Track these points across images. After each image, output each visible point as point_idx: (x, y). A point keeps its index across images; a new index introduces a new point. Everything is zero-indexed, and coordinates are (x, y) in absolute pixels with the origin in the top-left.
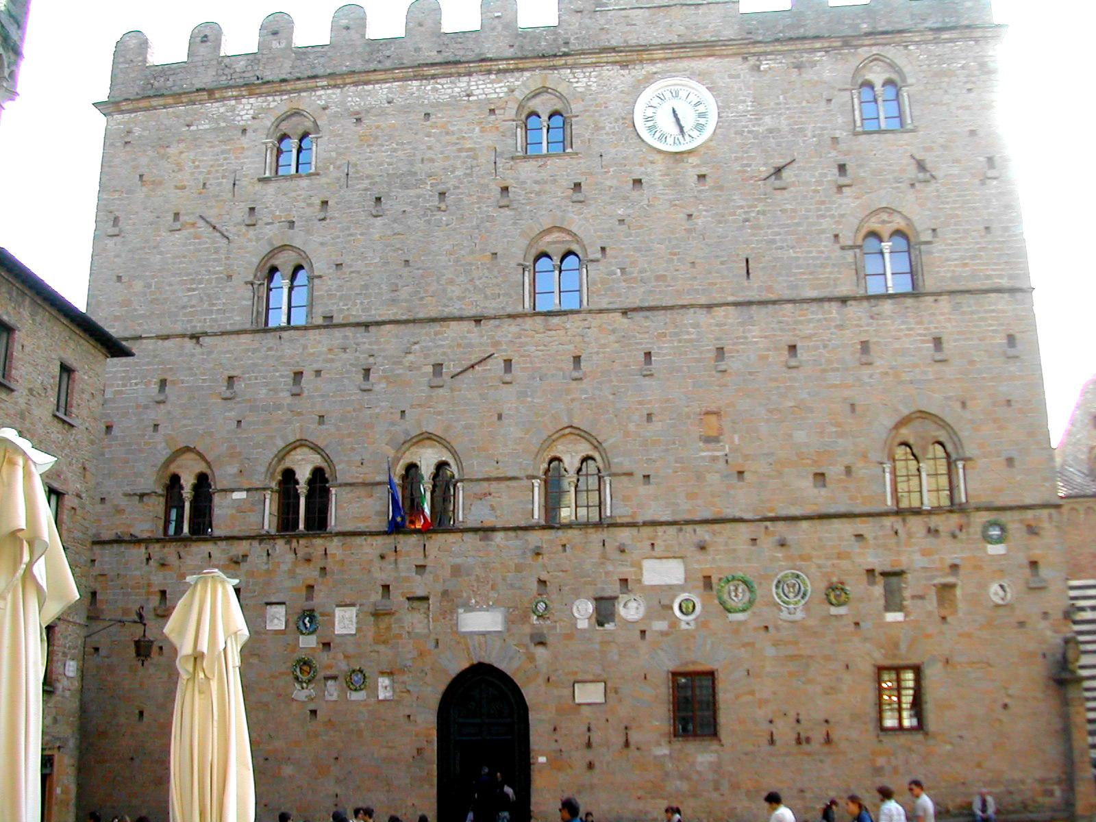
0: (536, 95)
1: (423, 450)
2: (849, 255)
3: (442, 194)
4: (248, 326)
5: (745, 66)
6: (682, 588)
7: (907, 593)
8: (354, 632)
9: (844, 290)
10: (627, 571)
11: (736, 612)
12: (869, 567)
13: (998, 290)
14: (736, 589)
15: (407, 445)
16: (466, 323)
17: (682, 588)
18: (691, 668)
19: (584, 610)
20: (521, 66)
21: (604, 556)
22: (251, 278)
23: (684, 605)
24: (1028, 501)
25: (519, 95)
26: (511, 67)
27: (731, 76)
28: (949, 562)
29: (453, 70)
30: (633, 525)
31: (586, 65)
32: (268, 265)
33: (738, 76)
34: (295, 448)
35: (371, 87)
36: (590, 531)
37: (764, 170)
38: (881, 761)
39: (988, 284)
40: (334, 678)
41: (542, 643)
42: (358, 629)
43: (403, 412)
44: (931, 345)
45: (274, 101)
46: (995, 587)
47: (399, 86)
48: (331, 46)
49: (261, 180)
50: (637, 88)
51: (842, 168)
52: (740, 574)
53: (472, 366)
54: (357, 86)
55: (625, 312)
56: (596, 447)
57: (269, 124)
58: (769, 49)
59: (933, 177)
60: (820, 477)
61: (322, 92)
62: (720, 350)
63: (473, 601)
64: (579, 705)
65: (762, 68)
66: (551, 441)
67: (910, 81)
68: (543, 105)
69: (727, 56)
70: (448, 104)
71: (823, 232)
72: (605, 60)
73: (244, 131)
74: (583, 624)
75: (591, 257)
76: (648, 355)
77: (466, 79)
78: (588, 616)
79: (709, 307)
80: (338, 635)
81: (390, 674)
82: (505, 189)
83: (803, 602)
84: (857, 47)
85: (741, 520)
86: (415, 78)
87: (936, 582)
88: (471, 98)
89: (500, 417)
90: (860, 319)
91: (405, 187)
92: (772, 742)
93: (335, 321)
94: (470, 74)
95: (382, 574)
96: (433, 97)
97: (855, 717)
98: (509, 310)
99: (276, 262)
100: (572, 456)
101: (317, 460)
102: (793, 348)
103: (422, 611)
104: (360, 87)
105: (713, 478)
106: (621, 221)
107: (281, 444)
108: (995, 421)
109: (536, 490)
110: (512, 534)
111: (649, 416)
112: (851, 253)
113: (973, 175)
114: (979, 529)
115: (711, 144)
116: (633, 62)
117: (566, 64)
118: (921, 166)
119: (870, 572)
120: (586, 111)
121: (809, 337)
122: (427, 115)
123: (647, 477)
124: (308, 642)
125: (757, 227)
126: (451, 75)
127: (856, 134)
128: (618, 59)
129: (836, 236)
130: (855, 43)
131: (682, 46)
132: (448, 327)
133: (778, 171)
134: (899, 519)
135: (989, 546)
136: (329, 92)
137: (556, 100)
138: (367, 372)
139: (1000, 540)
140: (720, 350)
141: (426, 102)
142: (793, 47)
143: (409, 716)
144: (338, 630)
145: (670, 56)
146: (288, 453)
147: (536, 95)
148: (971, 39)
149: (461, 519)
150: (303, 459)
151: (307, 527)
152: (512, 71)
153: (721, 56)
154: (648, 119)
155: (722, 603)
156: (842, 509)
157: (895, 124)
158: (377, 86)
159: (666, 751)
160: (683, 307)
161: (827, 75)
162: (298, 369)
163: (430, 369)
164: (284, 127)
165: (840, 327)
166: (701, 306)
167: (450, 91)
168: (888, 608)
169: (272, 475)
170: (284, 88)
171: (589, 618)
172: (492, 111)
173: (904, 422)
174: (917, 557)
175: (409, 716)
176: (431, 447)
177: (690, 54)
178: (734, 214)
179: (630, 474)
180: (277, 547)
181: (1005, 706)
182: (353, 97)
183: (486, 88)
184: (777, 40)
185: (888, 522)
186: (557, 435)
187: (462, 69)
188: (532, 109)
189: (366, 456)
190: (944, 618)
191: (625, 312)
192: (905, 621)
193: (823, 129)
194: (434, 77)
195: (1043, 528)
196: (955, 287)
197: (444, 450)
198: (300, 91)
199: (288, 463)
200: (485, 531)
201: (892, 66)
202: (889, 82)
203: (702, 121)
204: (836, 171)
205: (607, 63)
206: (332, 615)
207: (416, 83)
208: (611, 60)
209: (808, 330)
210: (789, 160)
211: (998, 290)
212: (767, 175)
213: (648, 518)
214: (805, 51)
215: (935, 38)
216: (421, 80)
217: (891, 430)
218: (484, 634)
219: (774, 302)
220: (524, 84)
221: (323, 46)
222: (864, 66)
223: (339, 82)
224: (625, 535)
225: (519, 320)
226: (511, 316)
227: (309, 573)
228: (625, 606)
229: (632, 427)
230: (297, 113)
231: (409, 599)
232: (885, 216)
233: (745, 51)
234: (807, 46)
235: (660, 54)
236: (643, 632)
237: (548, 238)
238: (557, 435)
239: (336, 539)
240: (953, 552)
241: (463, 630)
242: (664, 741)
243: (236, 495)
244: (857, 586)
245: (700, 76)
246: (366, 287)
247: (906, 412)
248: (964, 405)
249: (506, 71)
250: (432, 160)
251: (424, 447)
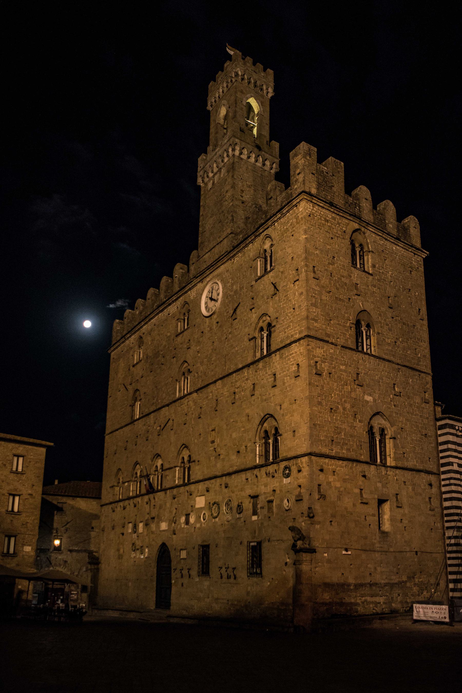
2: (252, 342)
7: (259, 506)
13: (295, 342)
19: (183, 519)
21: (188, 498)
24: (299, 453)
28: (272, 489)
37: (232, 312)
38: (249, 588)
39: (292, 339)
40: (138, 549)
46: (286, 501)
53: (166, 425)
55: (196, 391)
58: (235, 252)
72: (196, 282)
74: (183, 526)
79: (215, 382)
87: (268, 499)
92: (222, 577)
105: (212, 458)
109: (177, 472)
112: (252, 341)
114: (282, 471)
123: (198, 461)
124: (135, 536)
127: (256, 281)
133: (235, 310)
134: (258, 469)
135: (284, 479)
139: (288, 476)
156: (243, 467)
165: (247, 379)
174: (263, 487)
177: (215, 268)
179: (194, 461)
185: (256, 471)
190: (270, 517)
191: (196, 391)
192: (258, 520)
195: (303, 467)
196: (281, 345)
200: (165, 490)
206: (138, 526)
208: (197, 281)
211: (295, 342)
213: (197, 479)
217: (259, 425)
218: (164, 531)
224: (193, 487)
226: (175, 401)
232: (264, 318)
233: (229, 257)
235: (208, 272)
240: (274, 484)
243: (126, 484)
247: (262, 415)
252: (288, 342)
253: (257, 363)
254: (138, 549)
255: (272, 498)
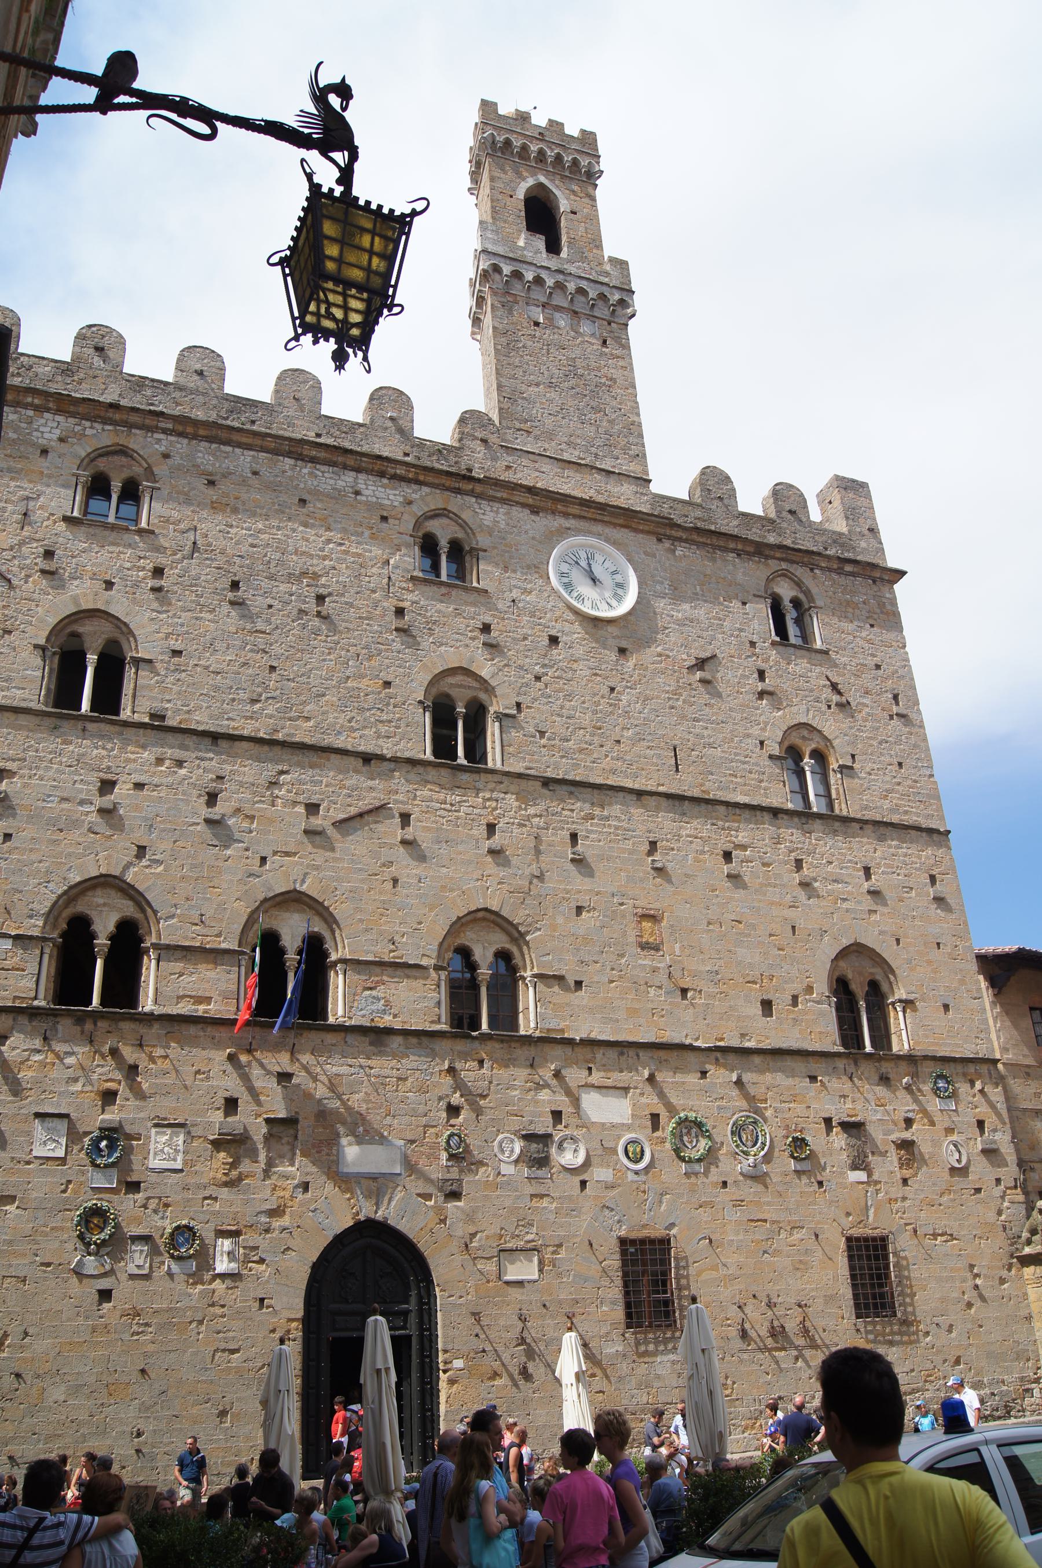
0: (435, 515)
1: (287, 915)
3: (320, 599)
4: (33, 705)
5: (660, 546)
6: (628, 1128)
8: (178, 1165)
9: (775, 802)
10: (562, 1101)
11: (690, 1161)
12: (827, 1115)
14: (689, 1133)
15: (267, 905)
16: (352, 759)
17: (628, 1128)
18: (645, 1233)
20: (421, 478)
22: (42, 641)
23: (630, 1149)
25: (418, 510)
26: (410, 476)
27: (646, 553)
29: (340, 459)
30: (570, 1042)
31: (492, 499)
32: (68, 630)
33: (654, 556)
34: (94, 887)
35: (229, 449)
36: (513, 1045)
41: (454, 1195)
42: (185, 1162)
43: (263, 860)
44: (862, 873)
45: (92, 427)
47: (266, 458)
48: (177, 387)
49: (66, 519)
50: (552, 538)
51: (761, 675)
52: (692, 1115)
53: (361, 815)
54: (211, 442)
56: (514, 940)
57: (84, 454)
59: (848, 703)
60: (767, 1006)
61: (162, 436)
62: (653, 844)
63: (361, 1129)
64: (507, 1283)
65: (677, 553)
66: (460, 924)
67: (819, 603)
68: (444, 532)
69: (642, 531)
70: (328, 496)
71: (748, 736)
73: (44, 452)
75: (507, 711)
76: (574, 837)
77: (353, 474)
78: (515, 1157)
80: (153, 1170)
81: (235, 1234)
82: (400, 612)
83: (762, 1153)
84: (767, 557)
85: (691, 1048)
86: (289, 454)
88: (358, 497)
89: (395, 881)
90: (792, 835)
91: (271, 578)
92: (744, 1334)
93: (170, 722)
94: (358, 470)
95: (231, 1084)
96: (311, 483)
97: (829, 1299)
98: (407, 754)
99: (85, 628)
100: (484, 948)
101: (129, 909)
102: (727, 856)
103: (285, 1140)
104: (214, 446)
106: (538, 678)
107: (76, 878)
108: (929, 962)
110: (414, 1040)
111: (579, 910)
113: (883, 710)
115: (632, 618)
116: (545, 510)
117: (472, 491)
118: (834, 687)
119: (828, 1121)
120: (495, 548)
121: (744, 847)
122: (303, 502)
123: (579, 984)
125: (683, 717)
126: (334, 464)
128: (530, 501)
129: (762, 743)
130: (767, 553)
131: (603, 507)
132: (329, 760)
136: (173, 438)
137: (457, 528)
138: (212, 798)
140: (653, 844)
141: (302, 486)
142: (709, 542)
143: (262, 1300)
144: (155, 1163)
145: (583, 514)
146: (83, 892)
147: (435, 515)
148: (870, 577)
149: (340, 1012)
150: (105, 905)
151: (103, 1003)
152: (409, 481)
153: (636, 531)
154: (562, 575)
155: (677, 1151)
157: (799, 641)
158: (238, 451)
159: (620, 1349)
160: (612, 788)
161: (740, 577)
162: (109, 777)
163: (301, 809)
164: (102, 464)
166: (631, 791)
167: (332, 482)
168: (855, 1167)
169: (56, 919)
170: (111, 415)
171: (516, 1161)
172: (384, 519)
173: (844, 954)
175: (262, 1300)
176: (298, 911)
177: (606, 519)
178: (658, 697)
179: (560, 979)
180: (60, 1027)
181: (976, 1287)
182: (205, 455)
183: (376, 491)
184: (696, 529)
186: (469, 918)
187: (350, 461)
188: (428, 529)
189: (209, 912)
190: (905, 1181)
193: (741, 630)
194: (313, 460)
197: (316, 918)
198: (131, 426)
199: (80, 907)
201: (799, 584)
202: (796, 603)
203: (620, 591)
204: (756, 675)
205: (517, 503)
207: (289, 461)
209: (742, 837)
210: (708, 654)
211: (919, 829)
212: (688, 664)
214: (720, 548)
215: (839, 568)
216: (297, 459)
219: (708, 801)
220: (422, 498)
221: (166, 384)
222: (773, 579)
223: (189, 430)
225: (420, 769)
227: (106, 1073)
228: (560, 1146)
229: (560, 920)
230: (123, 451)
231: (268, 1121)
232: (805, 733)
233: (662, 531)
234: (722, 543)
235: (575, 510)
236: (583, 1184)
237: (451, 680)
238: (469, 918)
239: (156, 1026)
241: (345, 1170)
242: (615, 1335)
244: (816, 1138)
245: (615, 543)
246: (216, 688)
247: (845, 942)
248: (898, 941)
249: (402, 479)
250: (311, 556)
251: (287, 910)
252: (895, 819)
253: (804, 820)
254: (146, 1239)
255: (907, 1135)
